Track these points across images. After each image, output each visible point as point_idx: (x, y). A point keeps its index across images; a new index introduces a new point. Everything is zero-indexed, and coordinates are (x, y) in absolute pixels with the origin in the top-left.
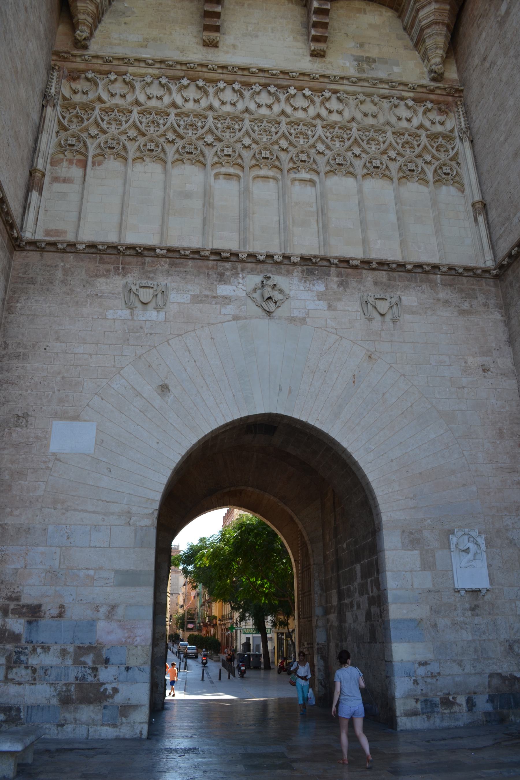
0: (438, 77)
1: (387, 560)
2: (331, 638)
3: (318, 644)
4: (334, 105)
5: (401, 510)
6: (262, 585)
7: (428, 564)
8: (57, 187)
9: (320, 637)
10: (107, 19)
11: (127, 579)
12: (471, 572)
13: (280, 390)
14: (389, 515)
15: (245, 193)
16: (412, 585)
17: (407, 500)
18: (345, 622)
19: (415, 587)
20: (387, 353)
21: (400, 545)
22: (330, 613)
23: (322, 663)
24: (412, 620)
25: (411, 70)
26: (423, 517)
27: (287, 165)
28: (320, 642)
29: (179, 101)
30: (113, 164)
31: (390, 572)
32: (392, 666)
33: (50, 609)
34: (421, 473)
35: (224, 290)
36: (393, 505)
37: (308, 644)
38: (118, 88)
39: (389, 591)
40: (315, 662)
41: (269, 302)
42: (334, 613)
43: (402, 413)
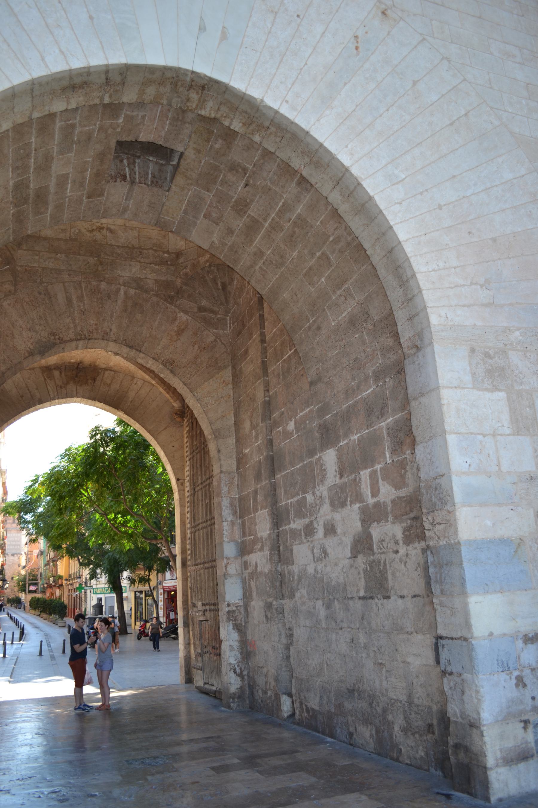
1: (445, 409)
2: (254, 594)
3: (229, 605)
5: (464, 306)
6: (124, 524)
9: (232, 593)
13: (202, 29)
14: (443, 314)
16: (499, 465)
17: (474, 287)
18: (290, 561)
19: (504, 468)
20: (414, 15)
21: (468, 378)
22: (250, 552)
23: (235, 635)
24: (504, 541)
26: (505, 324)
28: (232, 602)
31: (454, 436)
32: (471, 649)
34: (494, 240)
37: (203, 605)
39: (454, 478)
40: (223, 634)
42: (262, 549)
43: (452, 124)
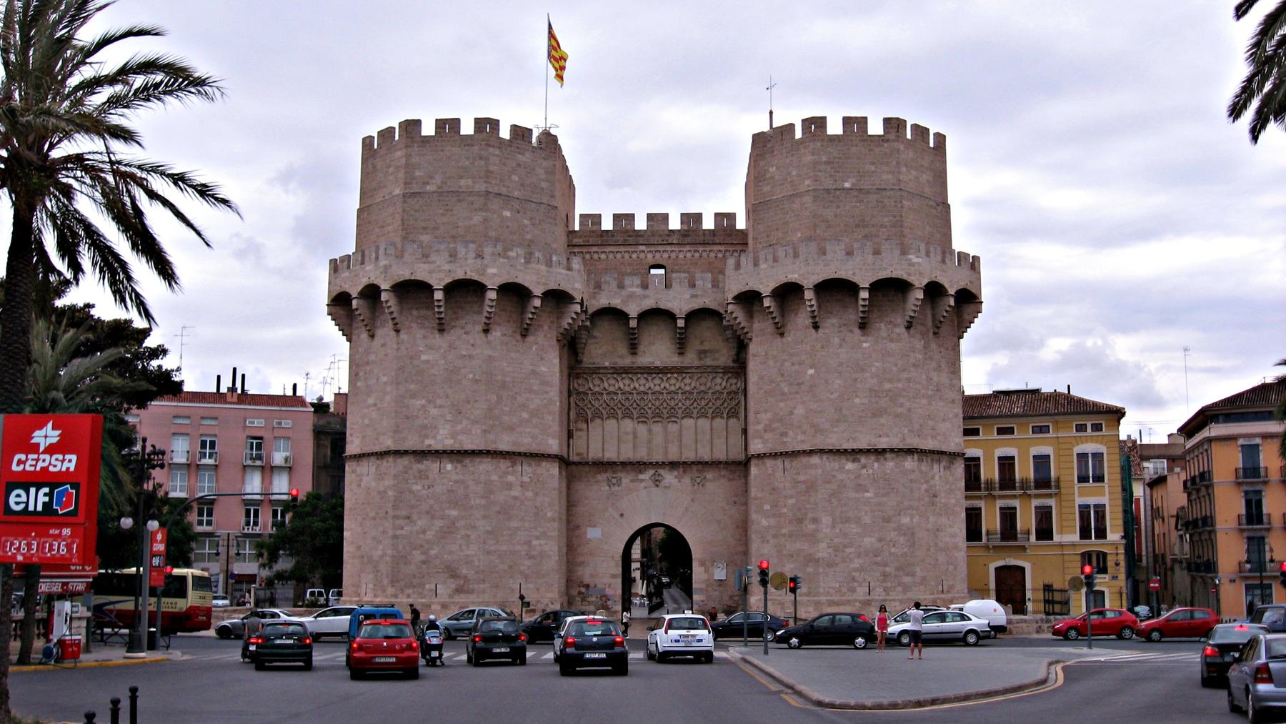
0: (734, 361)
4: (688, 381)
7: (707, 571)
8: (579, 433)
10: (590, 341)
11: (614, 576)
12: (720, 574)
15: (650, 431)
25: (724, 357)
27: (666, 415)
29: (621, 385)
30: (598, 421)
33: (592, 585)
35: (641, 477)
36: (696, 553)
38: (597, 382)
41: (657, 482)
